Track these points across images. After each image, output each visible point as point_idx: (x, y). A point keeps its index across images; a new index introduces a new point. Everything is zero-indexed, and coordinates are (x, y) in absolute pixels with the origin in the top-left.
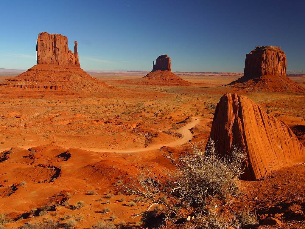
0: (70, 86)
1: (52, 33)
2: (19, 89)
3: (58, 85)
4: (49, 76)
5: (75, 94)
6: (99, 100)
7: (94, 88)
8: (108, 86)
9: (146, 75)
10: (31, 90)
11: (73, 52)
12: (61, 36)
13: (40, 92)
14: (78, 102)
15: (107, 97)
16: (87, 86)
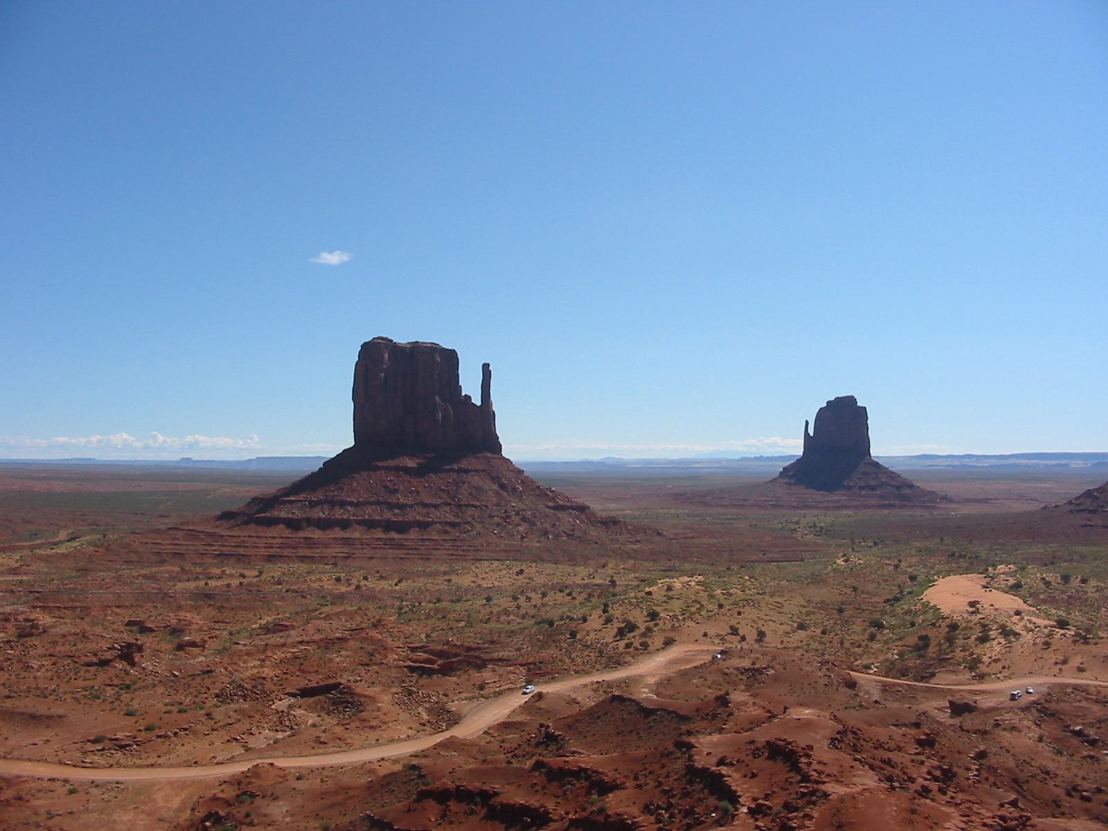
0: (451, 518)
1: (402, 338)
2: (280, 530)
3: (412, 516)
4: (388, 484)
5: (467, 548)
6: (521, 572)
7: (539, 524)
8: (596, 517)
9: (781, 473)
10: (317, 534)
11: (477, 400)
12: (434, 349)
13: (347, 541)
14: (447, 577)
15: (572, 560)
16: (516, 519)
